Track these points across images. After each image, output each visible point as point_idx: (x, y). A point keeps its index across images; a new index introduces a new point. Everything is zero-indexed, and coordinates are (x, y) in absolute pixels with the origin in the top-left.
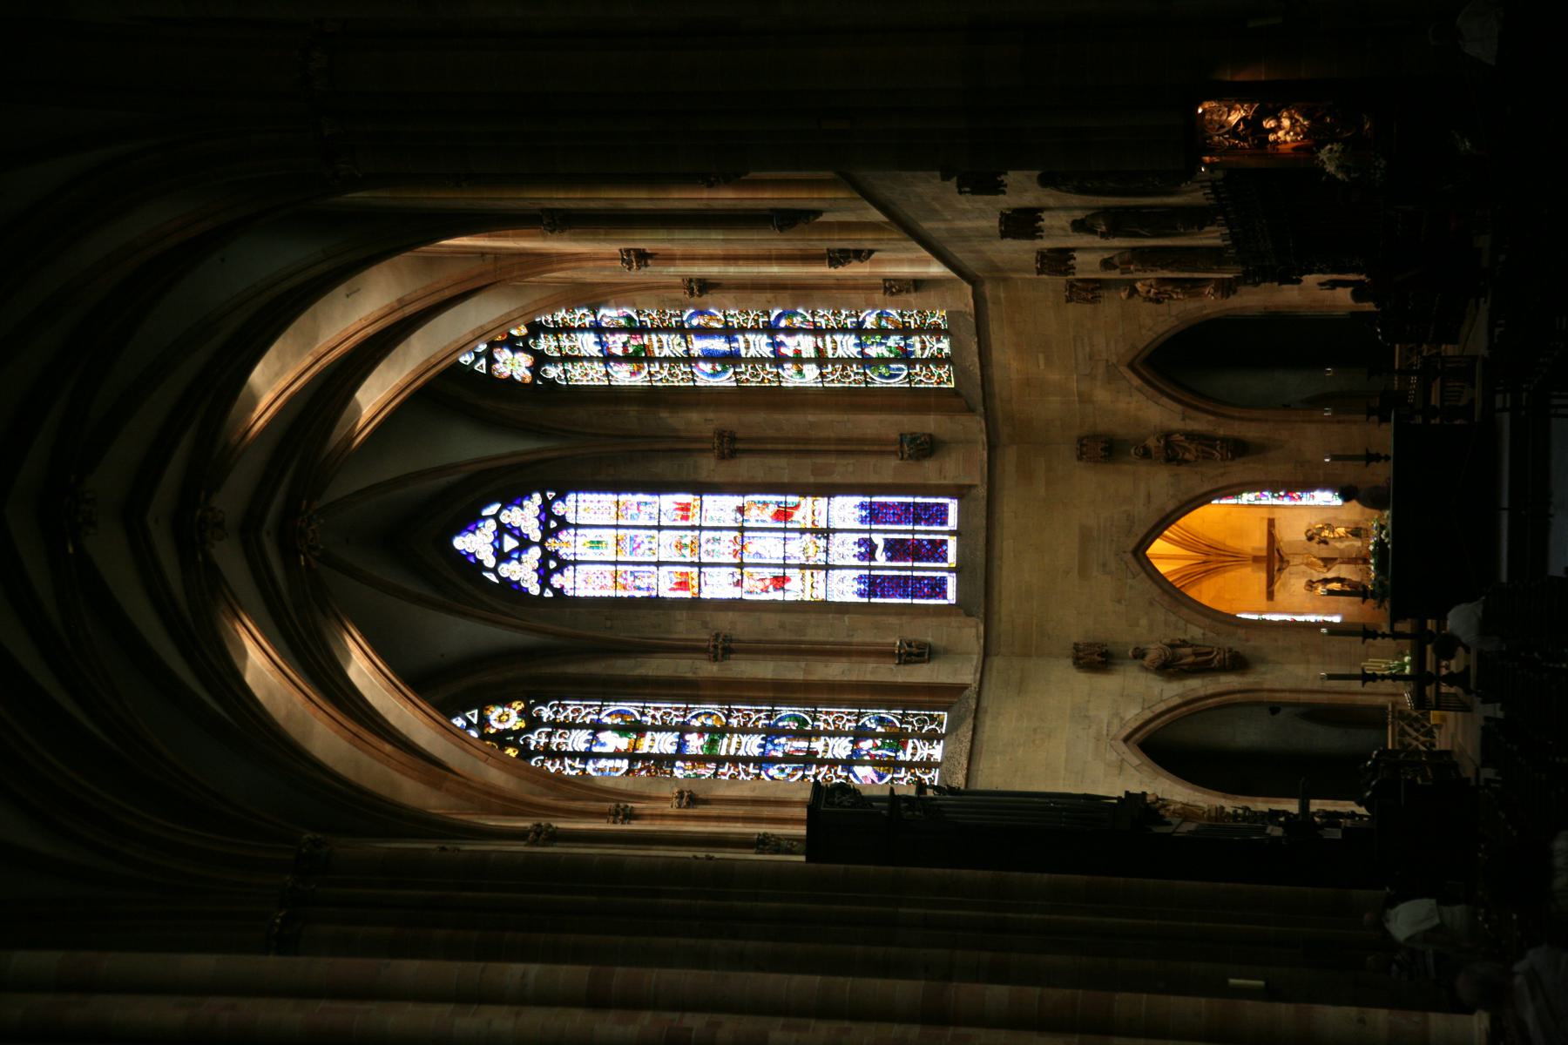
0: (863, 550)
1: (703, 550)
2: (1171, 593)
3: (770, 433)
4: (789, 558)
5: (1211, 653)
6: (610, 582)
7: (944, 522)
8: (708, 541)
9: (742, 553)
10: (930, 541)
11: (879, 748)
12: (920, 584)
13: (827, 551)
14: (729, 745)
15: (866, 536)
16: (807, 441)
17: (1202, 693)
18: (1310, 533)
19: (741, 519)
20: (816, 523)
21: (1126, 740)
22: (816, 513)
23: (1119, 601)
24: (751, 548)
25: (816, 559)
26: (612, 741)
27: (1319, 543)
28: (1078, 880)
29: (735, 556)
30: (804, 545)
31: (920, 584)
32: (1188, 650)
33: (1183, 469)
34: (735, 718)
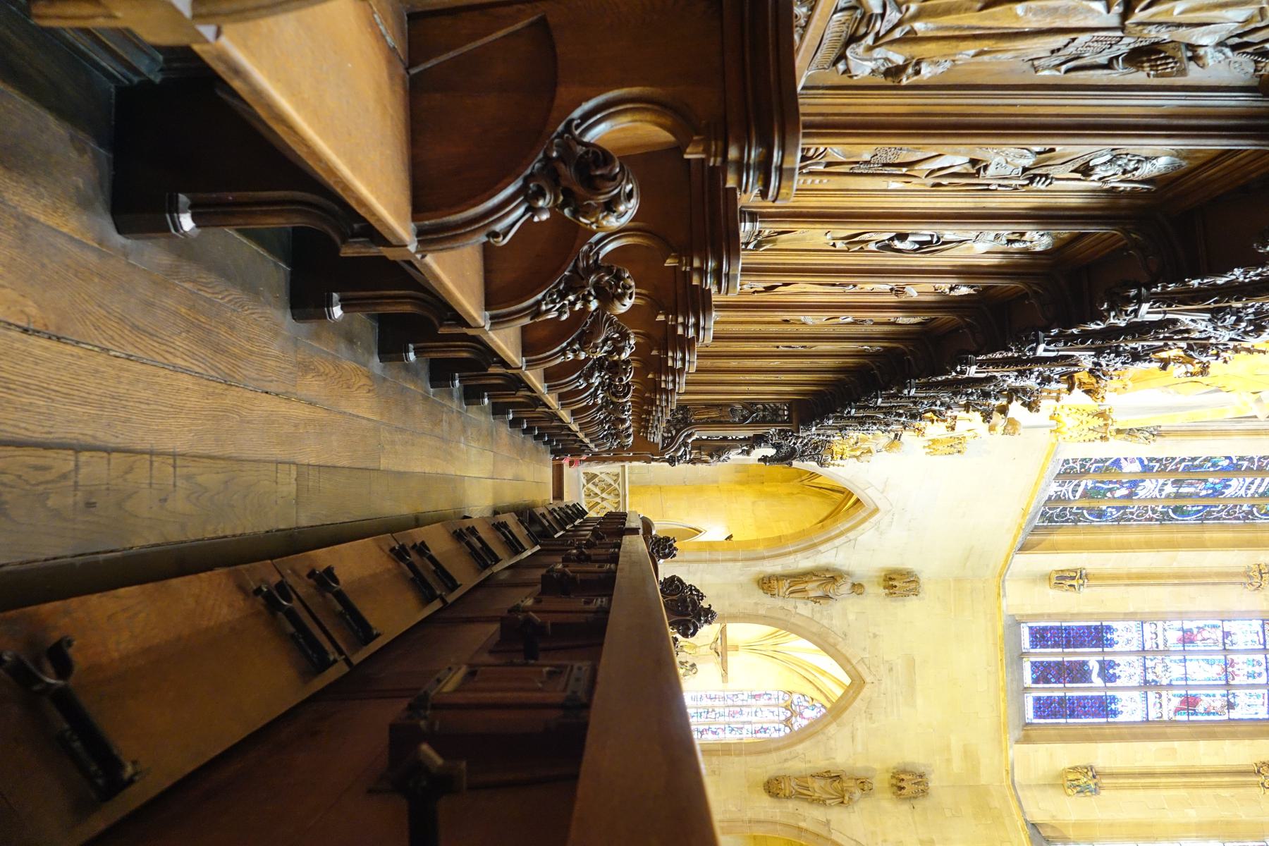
0: (1111, 671)
1: (1264, 666)
3: (1224, 793)
4: (1180, 661)
5: (791, 593)
7: (1037, 699)
8: (1260, 675)
9: (1226, 664)
10: (1048, 681)
11: (1110, 490)
12: (1055, 641)
13: (1145, 669)
14: (1260, 486)
15: (1109, 685)
16: (1186, 786)
17: (799, 555)
18: (694, 671)
19: (1230, 697)
20: (1158, 696)
21: (876, 510)
22: (1158, 705)
23: (875, 636)
24: (1217, 669)
25: (1155, 661)
27: (687, 662)
29: (1233, 660)
30: (1168, 674)
31: (1055, 641)
32: (812, 594)
33: (821, 764)
34: (1244, 511)
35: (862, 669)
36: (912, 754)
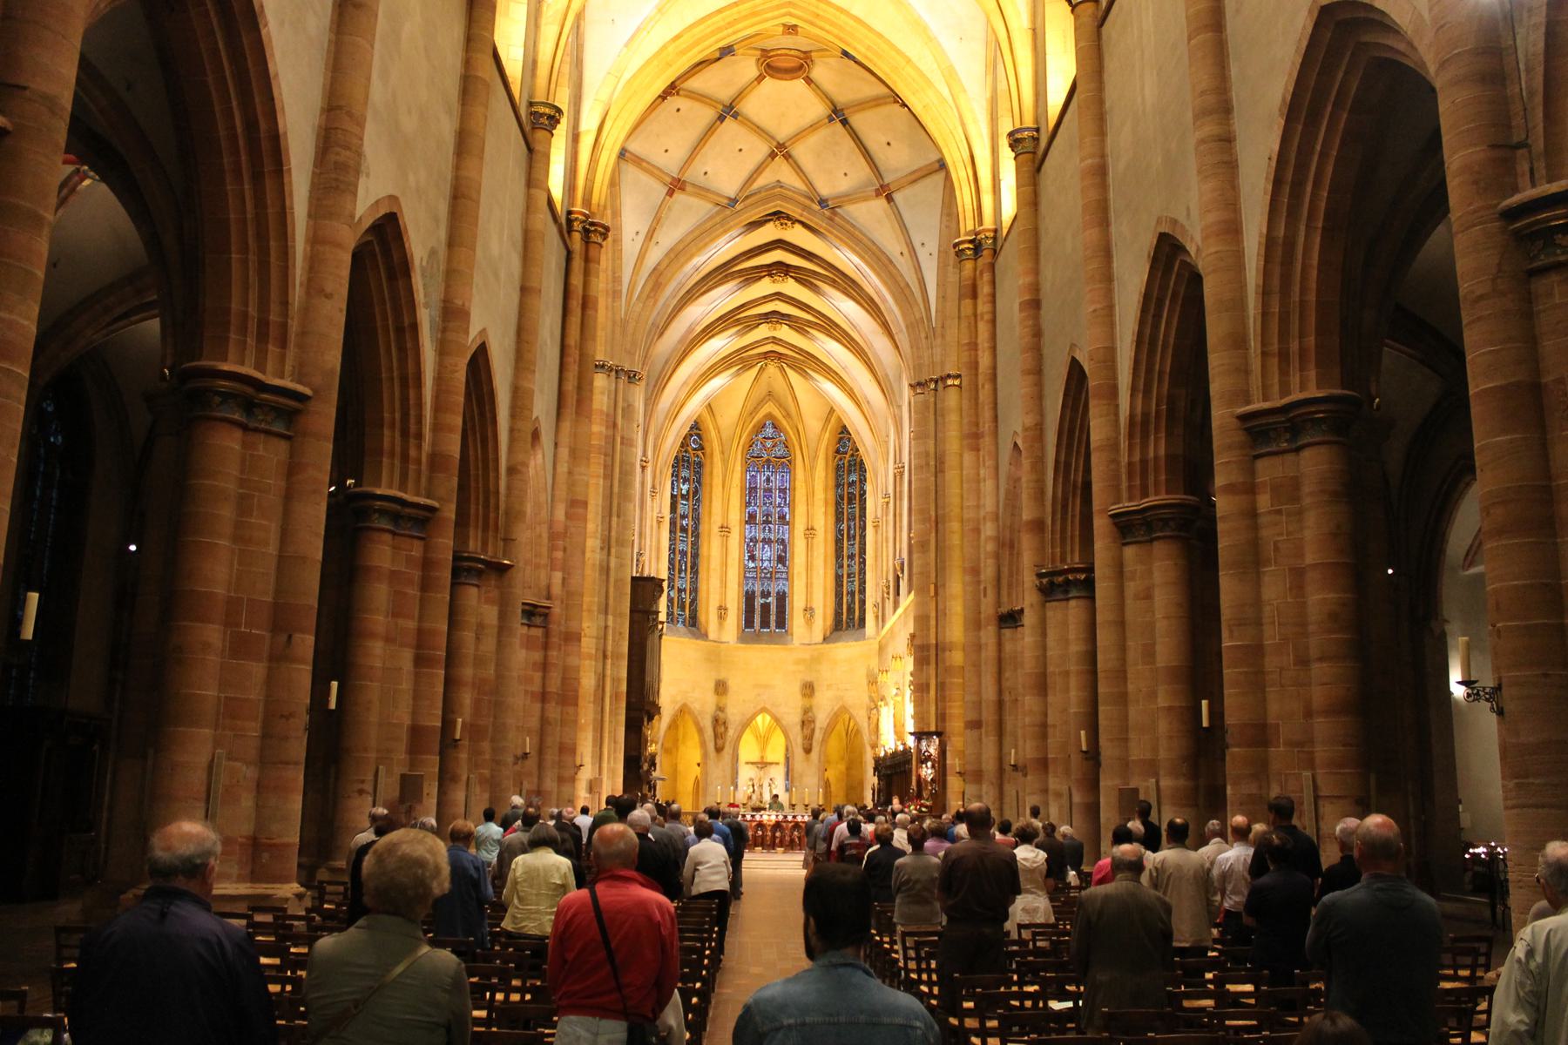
2: (747, 724)
3: (815, 554)
6: (753, 486)
26: (685, 488)
28: (624, 688)
32: (723, 729)
33: (799, 727)
35: (759, 708)
36: (796, 688)
